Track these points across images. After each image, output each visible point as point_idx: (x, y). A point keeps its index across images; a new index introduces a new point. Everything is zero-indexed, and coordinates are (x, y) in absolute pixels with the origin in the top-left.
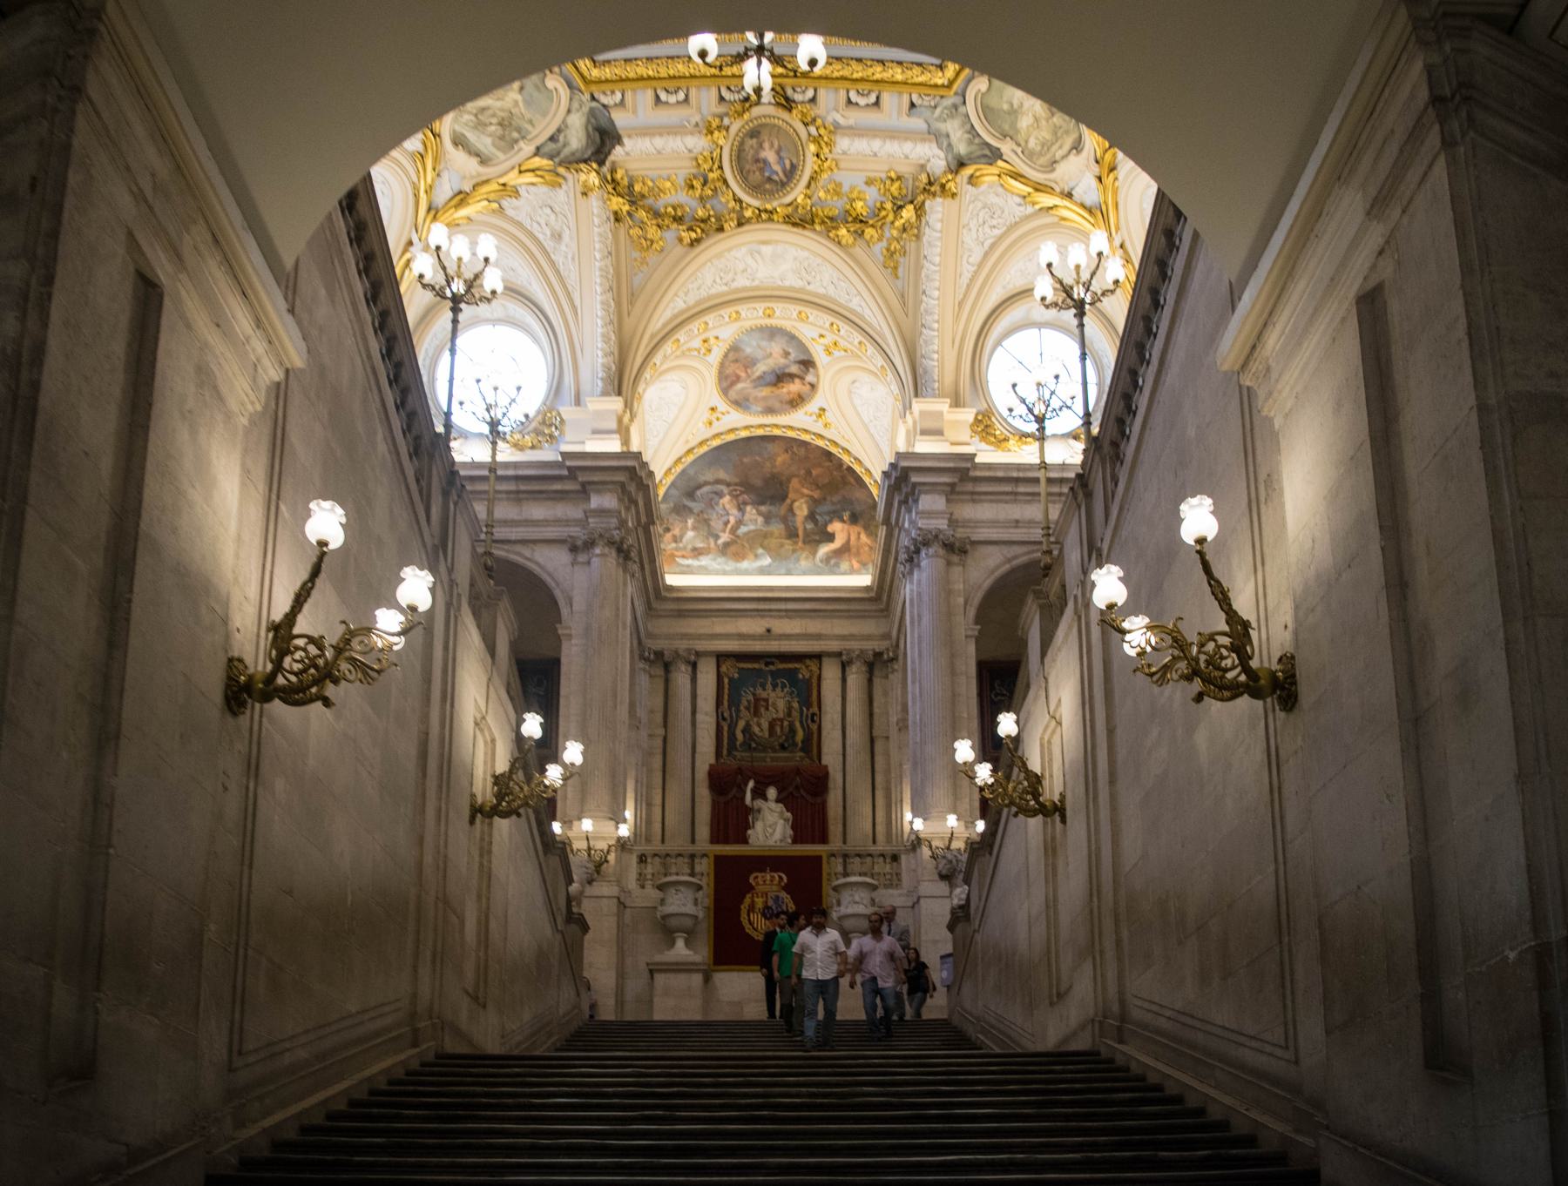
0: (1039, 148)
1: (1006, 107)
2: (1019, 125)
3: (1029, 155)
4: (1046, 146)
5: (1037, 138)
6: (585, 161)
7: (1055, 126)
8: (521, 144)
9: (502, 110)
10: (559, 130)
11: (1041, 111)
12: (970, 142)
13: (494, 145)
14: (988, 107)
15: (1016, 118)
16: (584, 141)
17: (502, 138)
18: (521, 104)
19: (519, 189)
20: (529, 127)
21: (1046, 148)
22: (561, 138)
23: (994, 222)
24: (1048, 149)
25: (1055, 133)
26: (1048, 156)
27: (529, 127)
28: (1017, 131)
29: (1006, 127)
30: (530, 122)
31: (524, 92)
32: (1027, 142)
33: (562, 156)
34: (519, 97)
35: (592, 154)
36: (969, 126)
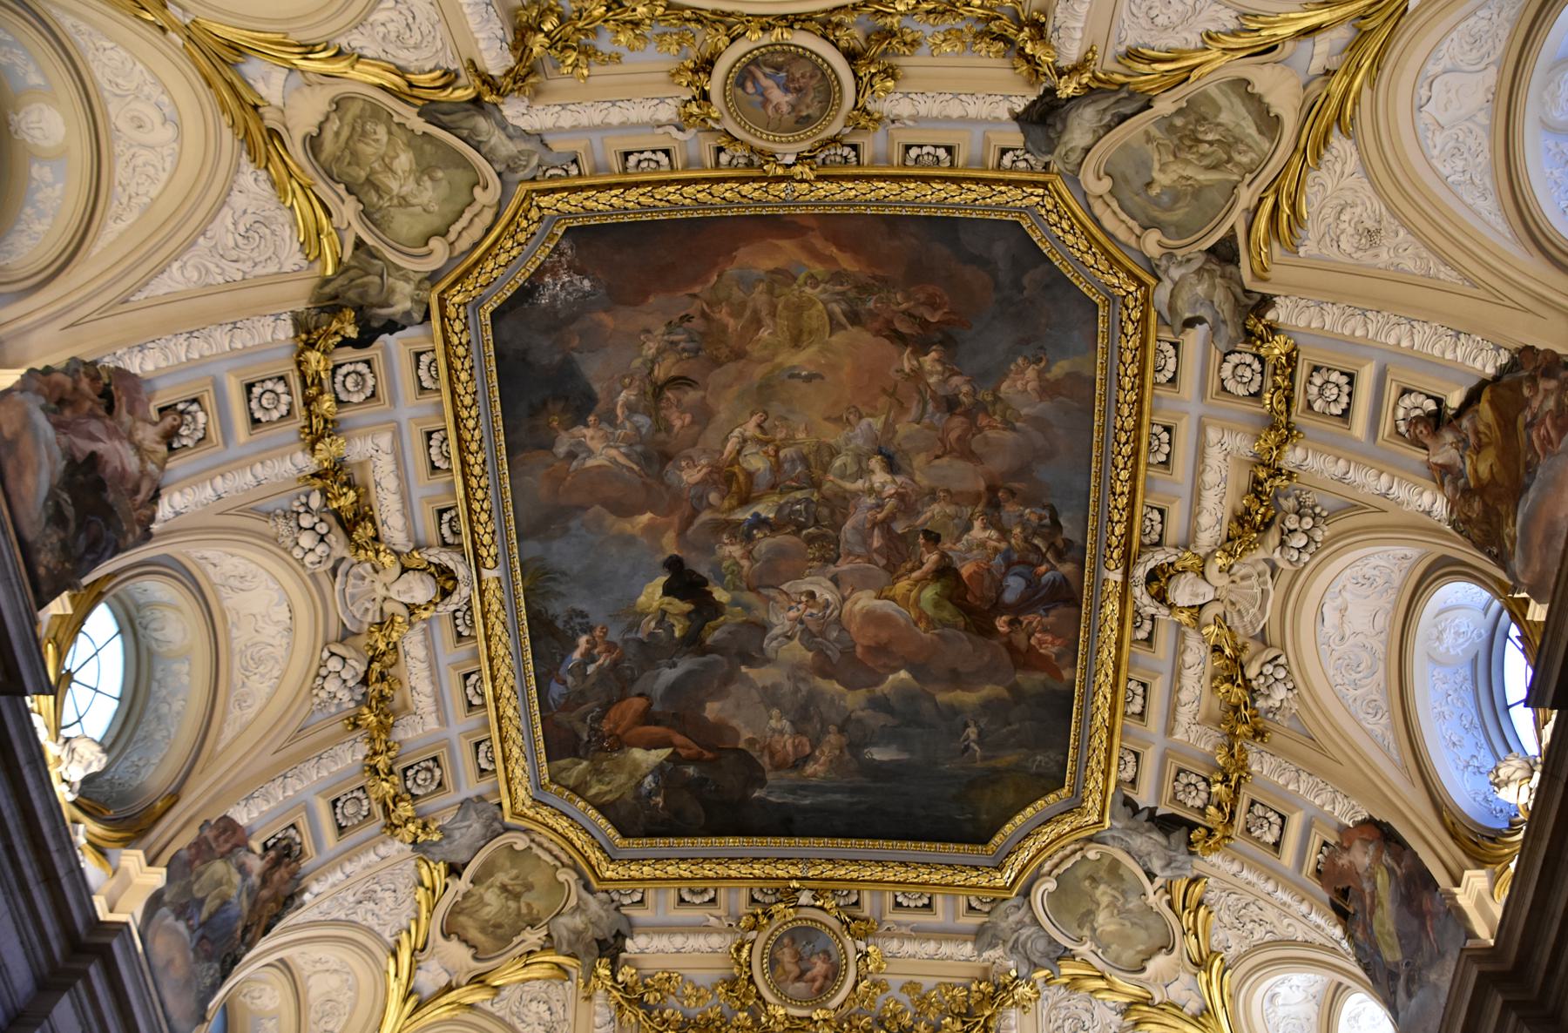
0: (369, 127)
1: (440, 174)
2: (411, 154)
3: (376, 113)
4: (359, 133)
5: (377, 141)
6: (1074, 97)
7: (358, 165)
8: (1171, 108)
9: (1188, 162)
10: (1109, 128)
11: (386, 180)
12: (473, 130)
13: (1219, 109)
14: (465, 168)
15: (418, 164)
16: (1073, 114)
17: (1202, 119)
18: (1156, 166)
19: (1200, 45)
20: (1155, 132)
21: (359, 129)
22: (1107, 118)
23: (391, 27)
24: (354, 128)
25: (354, 154)
26: (349, 118)
27: (1155, 132)
28: (409, 145)
29: (428, 148)
30: (1149, 138)
31: (1149, 180)
32: (390, 133)
33: (1112, 100)
34: (1156, 175)
35: (1063, 106)
36: (484, 149)
